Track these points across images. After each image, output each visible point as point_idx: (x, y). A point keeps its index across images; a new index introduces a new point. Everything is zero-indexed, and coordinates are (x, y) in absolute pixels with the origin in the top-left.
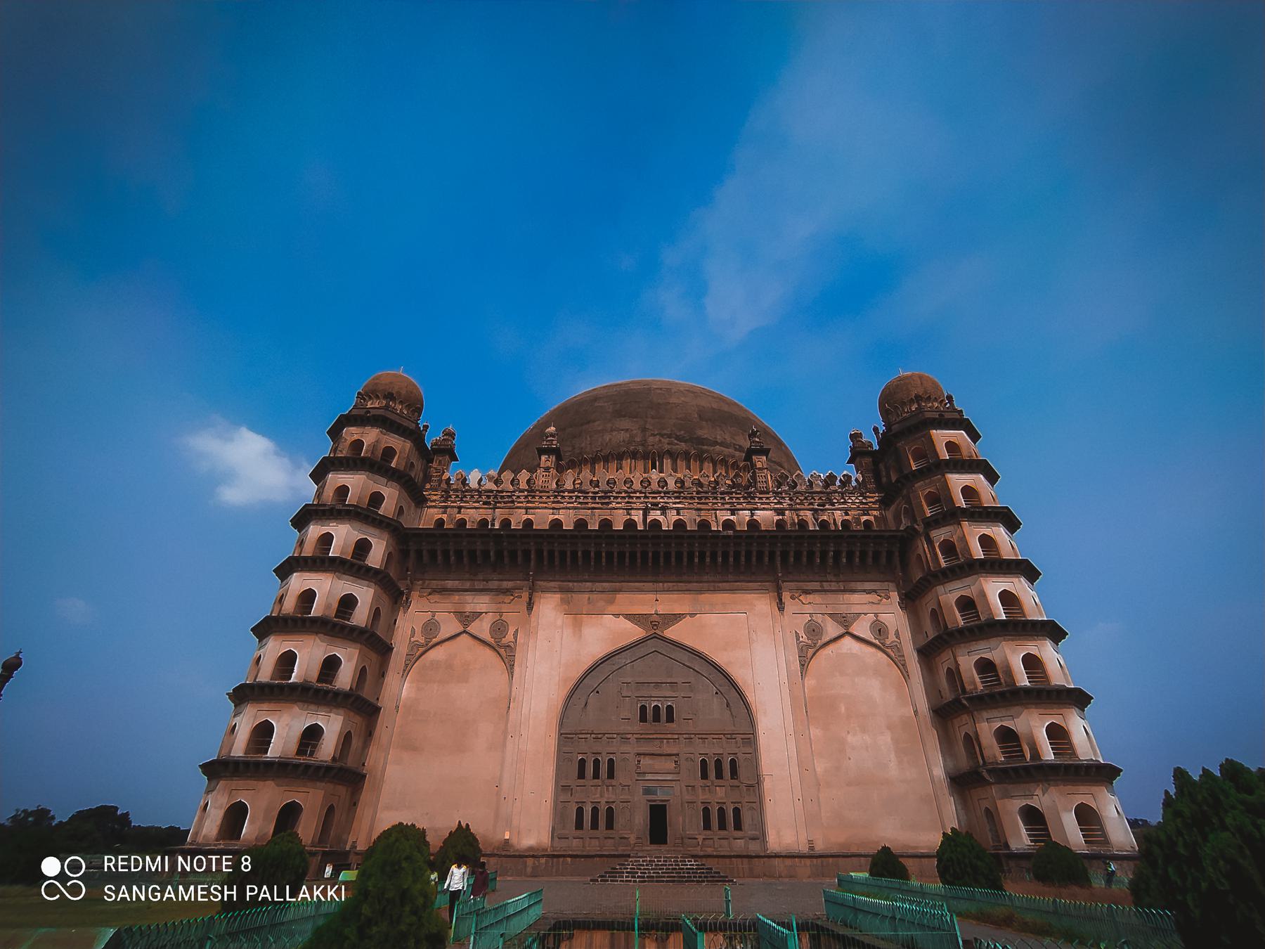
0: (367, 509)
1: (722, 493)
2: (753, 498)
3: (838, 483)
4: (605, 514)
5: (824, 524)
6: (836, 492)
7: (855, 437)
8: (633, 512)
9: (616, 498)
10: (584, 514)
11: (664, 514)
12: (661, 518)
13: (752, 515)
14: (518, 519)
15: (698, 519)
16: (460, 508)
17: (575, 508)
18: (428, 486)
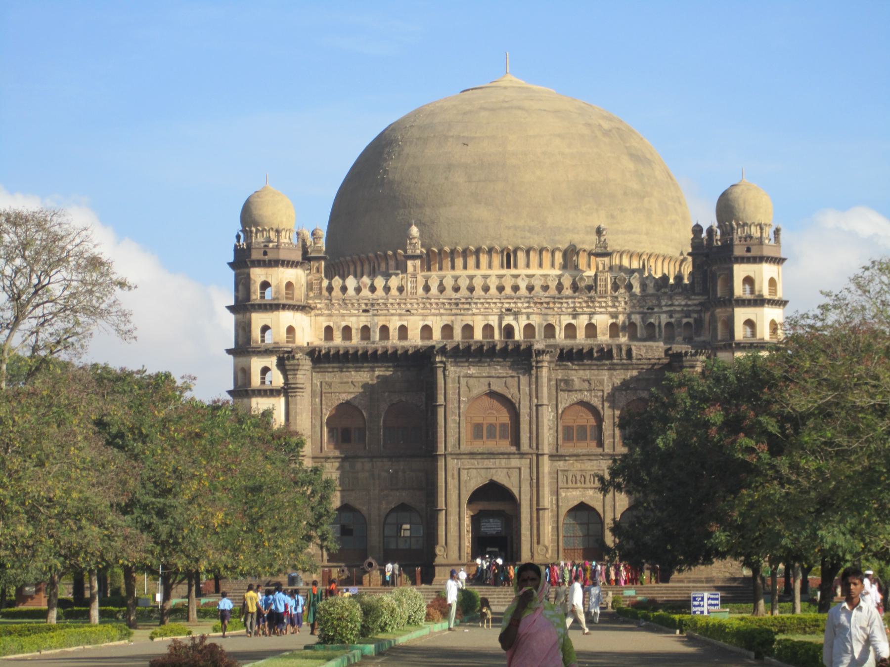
0: (288, 342)
1: (567, 298)
2: (593, 302)
3: (672, 281)
4: (468, 320)
5: (651, 325)
6: (665, 293)
7: (697, 229)
8: (490, 318)
9: (476, 303)
10: (446, 320)
11: (516, 319)
12: (513, 323)
13: (590, 319)
14: (394, 324)
15: (545, 324)
16: (343, 316)
17: (441, 315)
18: (312, 295)
